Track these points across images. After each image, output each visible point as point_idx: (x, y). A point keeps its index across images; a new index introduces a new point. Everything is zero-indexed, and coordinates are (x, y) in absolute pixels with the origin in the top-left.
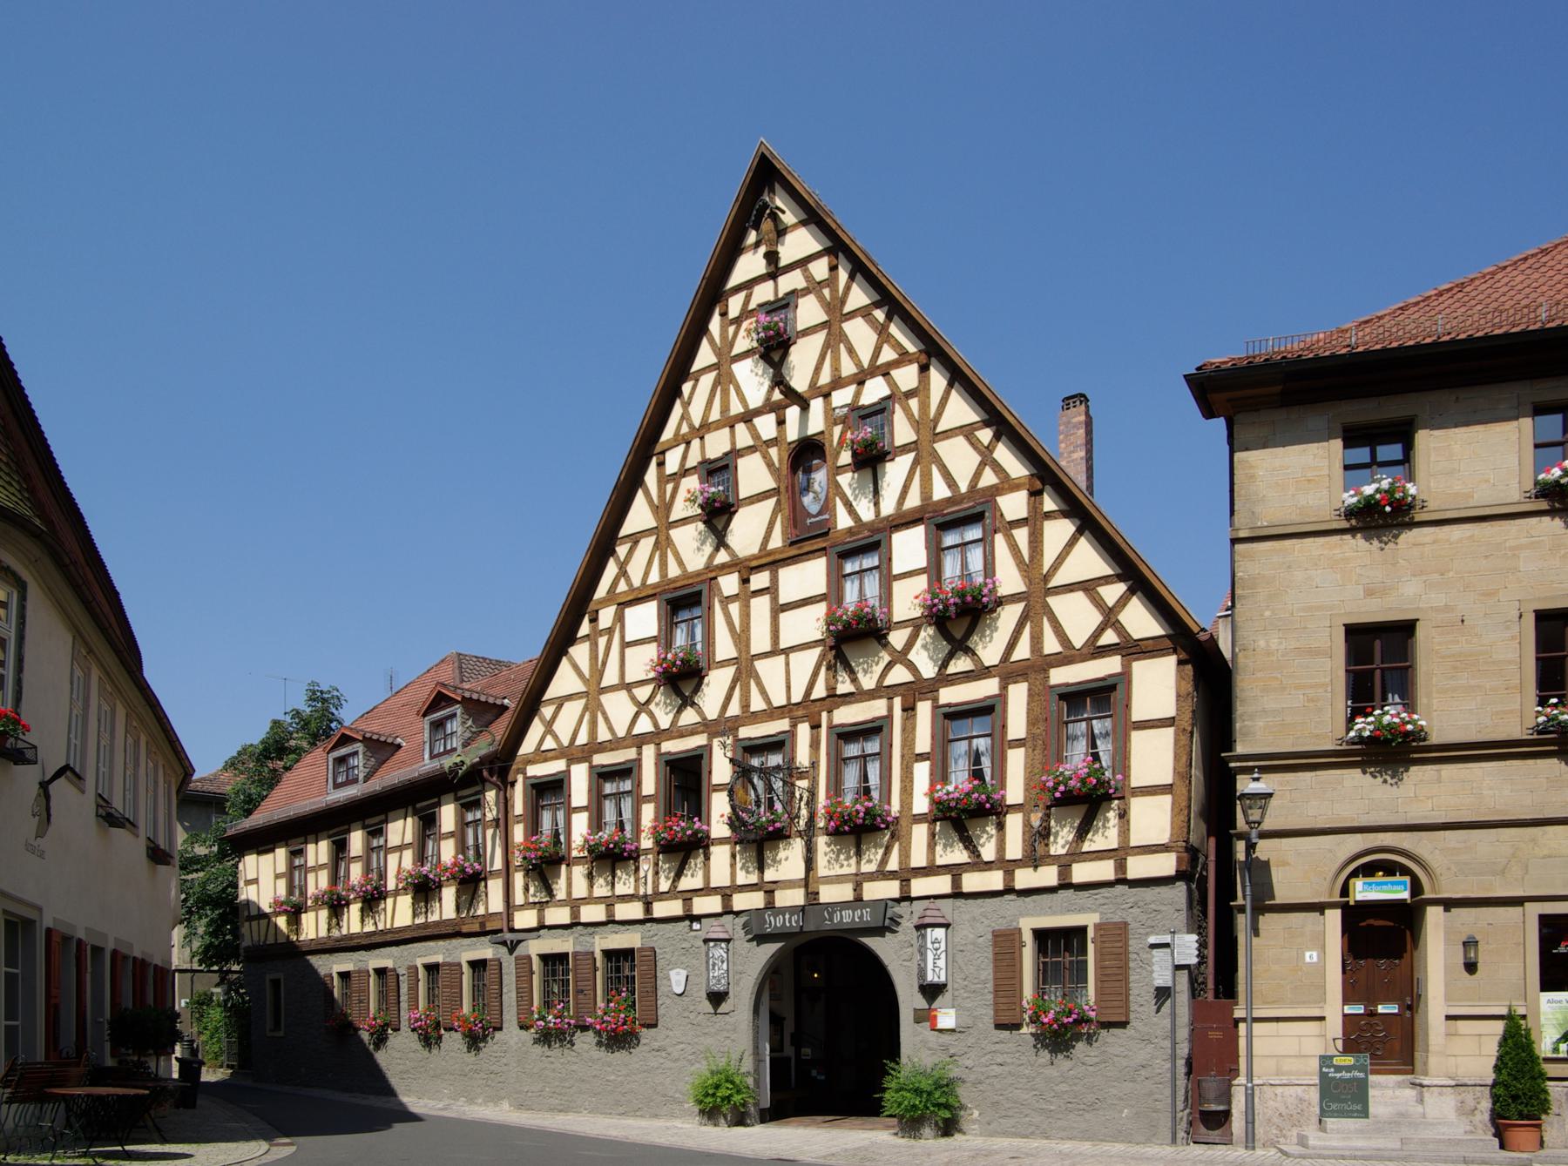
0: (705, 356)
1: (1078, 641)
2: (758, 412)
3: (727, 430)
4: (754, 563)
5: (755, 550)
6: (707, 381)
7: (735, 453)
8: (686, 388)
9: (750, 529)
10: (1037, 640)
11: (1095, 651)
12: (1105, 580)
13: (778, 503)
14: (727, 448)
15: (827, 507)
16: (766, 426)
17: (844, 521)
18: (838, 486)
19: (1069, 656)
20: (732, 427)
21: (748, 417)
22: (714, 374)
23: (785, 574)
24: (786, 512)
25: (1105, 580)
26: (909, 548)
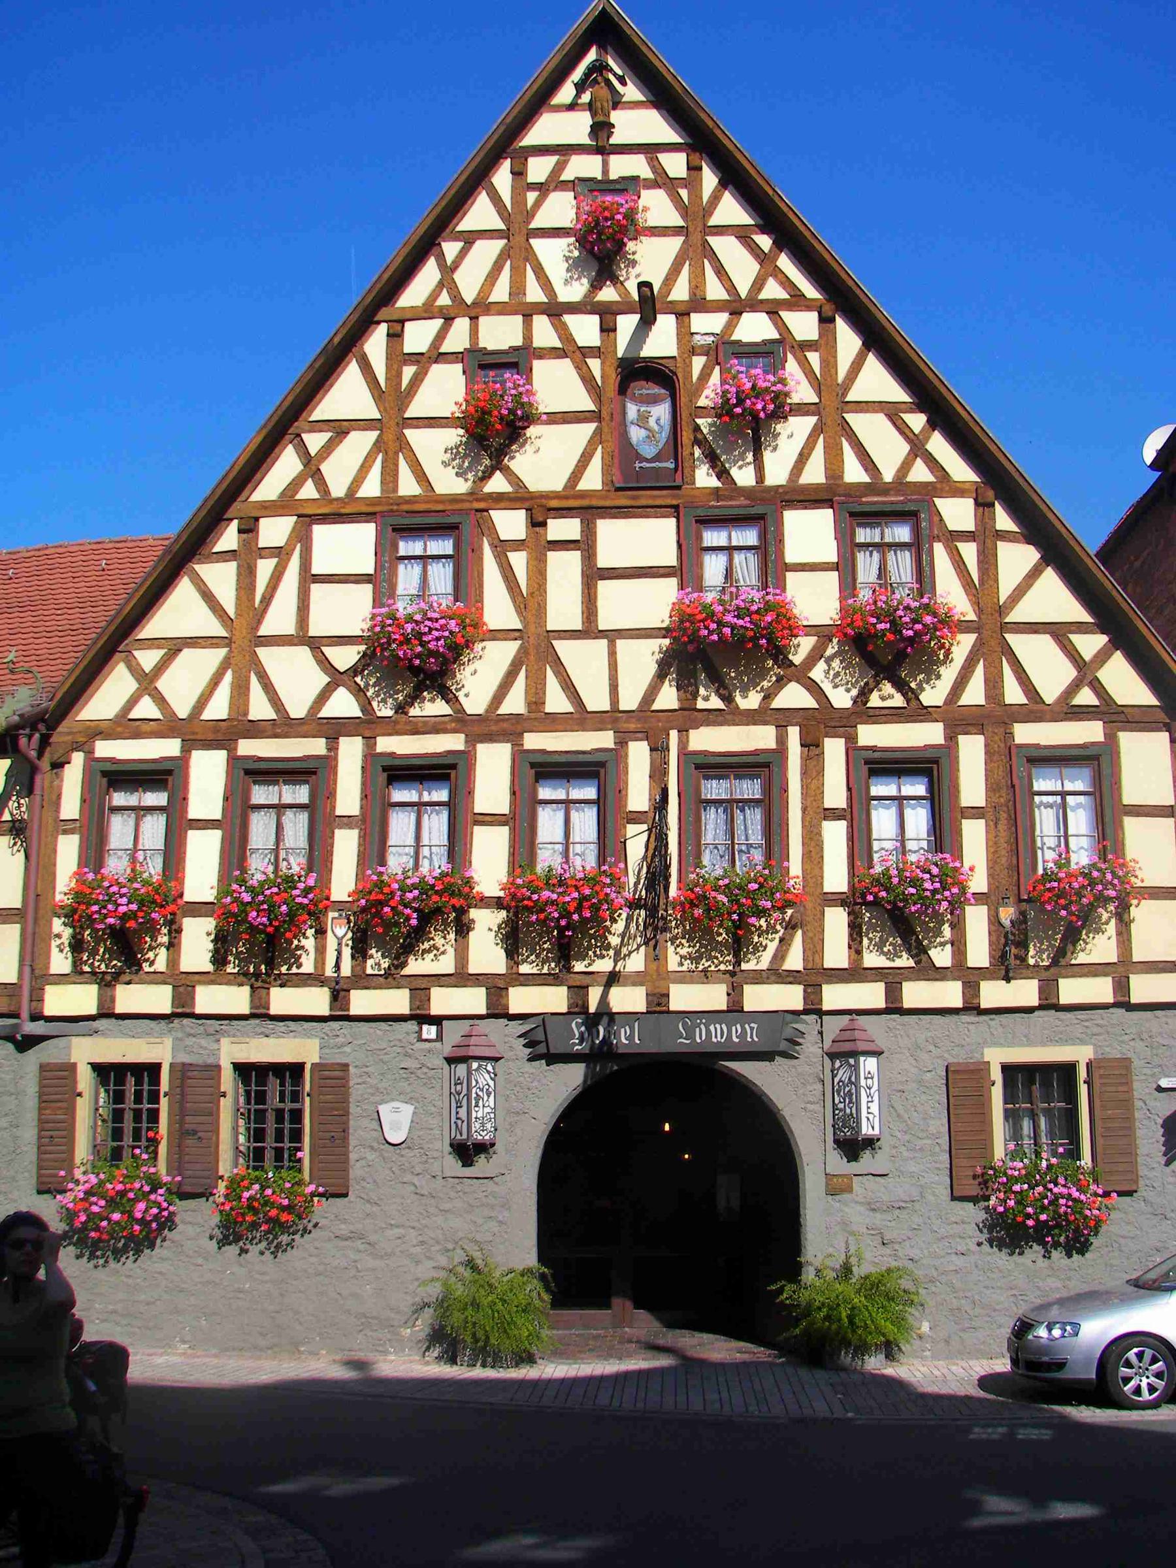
0: (480, 214)
4: (554, 503)
5: (558, 485)
9: (548, 459)
10: (994, 685)
11: (1067, 711)
12: (1080, 627)
13: (598, 433)
19: (1036, 709)
20: (528, 318)
21: (555, 310)
23: (605, 528)
24: (611, 446)
25: (1080, 627)
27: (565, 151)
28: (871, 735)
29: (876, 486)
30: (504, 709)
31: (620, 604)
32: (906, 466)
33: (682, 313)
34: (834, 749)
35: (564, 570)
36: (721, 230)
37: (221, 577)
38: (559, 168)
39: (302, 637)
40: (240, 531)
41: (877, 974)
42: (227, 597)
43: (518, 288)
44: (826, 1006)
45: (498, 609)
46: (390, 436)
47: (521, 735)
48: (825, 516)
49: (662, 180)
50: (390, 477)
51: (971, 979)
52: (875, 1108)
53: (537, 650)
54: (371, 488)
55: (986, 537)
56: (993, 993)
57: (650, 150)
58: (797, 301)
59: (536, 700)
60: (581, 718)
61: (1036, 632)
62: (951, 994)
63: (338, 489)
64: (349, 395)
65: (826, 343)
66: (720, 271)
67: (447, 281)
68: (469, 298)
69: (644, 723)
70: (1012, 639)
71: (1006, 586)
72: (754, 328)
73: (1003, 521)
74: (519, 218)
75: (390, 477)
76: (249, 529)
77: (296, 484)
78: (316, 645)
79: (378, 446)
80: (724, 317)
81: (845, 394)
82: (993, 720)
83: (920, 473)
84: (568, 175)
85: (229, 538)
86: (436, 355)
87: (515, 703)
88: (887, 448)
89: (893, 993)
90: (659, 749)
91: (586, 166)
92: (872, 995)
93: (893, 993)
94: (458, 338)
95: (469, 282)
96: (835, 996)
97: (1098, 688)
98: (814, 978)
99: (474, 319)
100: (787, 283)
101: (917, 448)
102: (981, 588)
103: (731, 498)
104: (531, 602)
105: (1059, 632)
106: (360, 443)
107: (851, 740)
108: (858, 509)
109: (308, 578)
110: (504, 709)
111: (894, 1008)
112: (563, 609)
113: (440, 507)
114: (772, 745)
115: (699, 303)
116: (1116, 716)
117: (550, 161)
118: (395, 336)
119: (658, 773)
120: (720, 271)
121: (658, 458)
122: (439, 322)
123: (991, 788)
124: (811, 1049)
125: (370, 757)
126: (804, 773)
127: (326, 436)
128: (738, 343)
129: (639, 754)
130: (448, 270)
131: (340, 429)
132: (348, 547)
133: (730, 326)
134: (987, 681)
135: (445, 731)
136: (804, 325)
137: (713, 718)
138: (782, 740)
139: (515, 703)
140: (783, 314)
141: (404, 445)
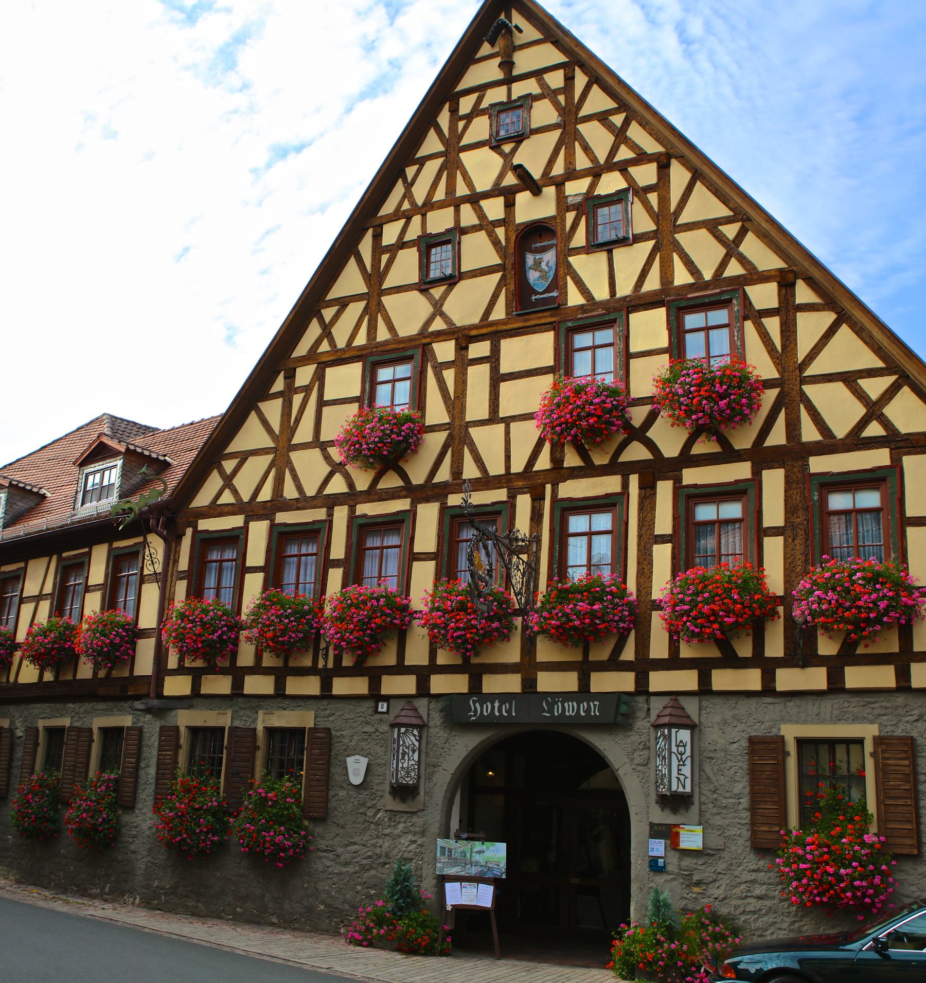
2: (486, 195)
3: (452, 209)
4: (474, 333)
5: (476, 320)
6: (432, 166)
7: (460, 230)
8: (410, 171)
10: (793, 427)
14: (451, 224)
15: (557, 284)
16: (494, 208)
17: (575, 298)
18: (569, 265)
21: (474, 199)
22: (441, 160)
23: (506, 345)
24: (512, 287)
26: (649, 329)
28: (692, 476)
29: (699, 284)
30: (436, 480)
31: (514, 397)
34: (664, 489)
36: (588, 118)
38: (479, 100)
39: (318, 443)
40: (285, 378)
48: (660, 314)
50: (372, 330)
55: (787, 310)
58: (642, 158)
59: (457, 471)
61: (830, 381)
63: (341, 343)
64: (351, 281)
66: (587, 149)
69: (529, 482)
71: (803, 348)
72: (611, 183)
73: (803, 294)
74: (454, 141)
75: (372, 330)
76: (290, 376)
77: (318, 343)
79: (366, 311)
81: (676, 220)
83: (734, 269)
84: (484, 104)
86: (401, 244)
90: (538, 498)
91: (497, 95)
92: (687, 680)
94: (414, 232)
96: (659, 681)
98: (643, 667)
99: (424, 215)
100: (634, 146)
101: (732, 249)
102: (783, 354)
103: (592, 311)
106: (355, 309)
107: (678, 480)
108: (684, 304)
110: (436, 480)
111: (705, 690)
113: (402, 346)
114: (618, 489)
115: (572, 174)
117: (473, 97)
118: (378, 237)
119: (536, 517)
120: (587, 149)
122: (403, 221)
125: (352, 517)
126: (641, 509)
127: (335, 309)
128: (599, 196)
129: (524, 503)
130: (409, 186)
131: (343, 303)
132: (345, 380)
133: (593, 186)
135: (399, 497)
136: (646, 174)
137: (575, 473)
138: (625, 485)
141: (380, 307)
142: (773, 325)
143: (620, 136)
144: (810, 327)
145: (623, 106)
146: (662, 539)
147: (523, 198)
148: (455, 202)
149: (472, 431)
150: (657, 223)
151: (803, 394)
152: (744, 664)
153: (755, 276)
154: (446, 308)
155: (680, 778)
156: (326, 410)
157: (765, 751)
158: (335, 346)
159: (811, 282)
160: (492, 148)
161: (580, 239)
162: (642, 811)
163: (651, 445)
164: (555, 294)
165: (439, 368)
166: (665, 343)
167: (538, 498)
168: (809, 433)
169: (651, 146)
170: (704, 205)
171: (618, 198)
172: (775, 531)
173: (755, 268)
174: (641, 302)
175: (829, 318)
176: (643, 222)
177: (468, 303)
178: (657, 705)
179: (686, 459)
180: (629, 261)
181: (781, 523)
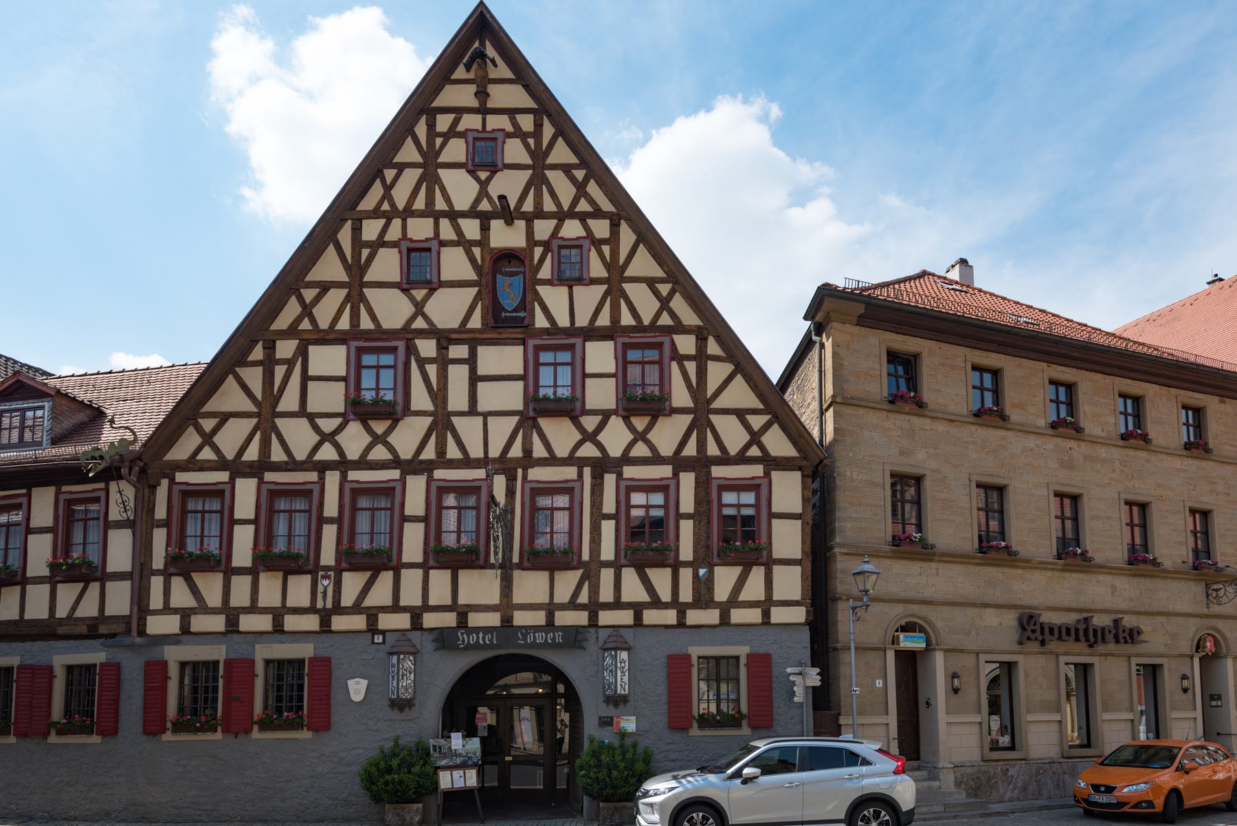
0: (407, 152)
1: (733, 450)
2: (464, 215)
4: (454, 336)
5: (455, 324)
10: (702, 445)
11: (742, 458)
13: (479, 293)
16: (471, 228)
17: (541, 322)
19: (725, 459)
21: (453, 215)
23: (482, 351)
24: (486, 302)
26: (601, 356)
27: (459, 111)
32: (658, 315)
33: (529, 219)
34: (610, 480)
35: (458, 376)
36: (554, 167)
37: (254, 377)
38: (456, 122)
39: (302, 412)
41: (630, 605)
42: (257, 389)
43: (430, 201)
44: (600, 623)
45: (421, 399)
46: (355, 293)
47: (432, 471)
49: (518, 133)
51: (682, 609)
52: (626, 679)
53: (442, 423)
54: (344, 324)
55: (702, 358)
56: (694, 617)
57: (512, 112)
58: (598, 213)
59: (441, 451)
60: (467, 462)
62: (670, 617)
63: (324, 324)
64: (330, 268)
65: (614, 239)
66: (553, 194)
67: (387, 195)
68: (401, 206)
70: (713, 418)
71: (711, 389)
72: (572, 229)
73: (713, 348)
75: (355, 317)
76: (270, 347)
77: (298, 320)
78: (311, 418)
79: (348, 298)
80: (554, 222)
81: (623, 272)
82: (701, 464)
83: (665, 320)
84: (460, 128)
85: (258, 353)
86: (381, 243)
87: (429, 453)
88: (646, 304)
89: (638, 617)
90: (511, 479)
91: (471, 122)
93: (638, 617)
94: (394, 233)
95: (401, 195)
96: (606, 618)
97: (762, 448)
100: (591, 201)
101: (665, 303)
102: (698, 390)
104: (439, 395)
105: (741, 414)
106: (335, 297)
107: (620, 475)
109: (306, 378)
110: (423, 457)
112: (457, 398)
115: (539, 213)
116: (772, 463)
117: (450, 117)
118: (357, 230)
119: (510, 493)
120: (553, 194)
121: (515, 310)
122: (383, 221)
123: (698, 502)
124: (592, 647)
126: (593, 493)
130: (388, 188)
131: (325, 287)
134: (698, 441)
136: (601, 228)
138: (580, 475)
139: (429, 453)
140: (589, 221)
142: (691, 367)
143: (581, 188)
144: (717, 372)
145: (583, 164)
146: (608, 517)
147: (496, 225)
148: (437, 216)
149: (454, 419)
150: (608, 272)
151: (709, 421)
152: (666, 606)
153: (679, 328)
154: (427, 309)
155: (622, 683)
156: (310, 384)
157: (678, 666)
158: (317, 326)
159: (718, 339)
160: (469, 172)
161: (545, 272)
162: (592, 709)
163: (600, 446)
164: (522, 314)
165: (422, 362)
166: (612, 370)
167: (511, 479)
168: (713, 450)
169: (607, 206)
170: (643, 264)
171: (575, 244)
172: (688, 516)
173: (680, 322)
174: (592, 333)
175: (730, 368)
176: (597, 269)
177: (449, 308)
178: (603, 634)
179: (626, 459)
180: (587, 298)
181: (692, 511)
